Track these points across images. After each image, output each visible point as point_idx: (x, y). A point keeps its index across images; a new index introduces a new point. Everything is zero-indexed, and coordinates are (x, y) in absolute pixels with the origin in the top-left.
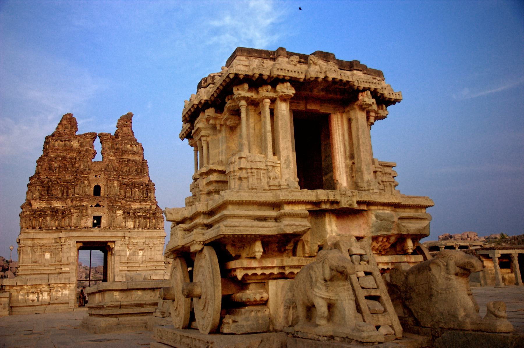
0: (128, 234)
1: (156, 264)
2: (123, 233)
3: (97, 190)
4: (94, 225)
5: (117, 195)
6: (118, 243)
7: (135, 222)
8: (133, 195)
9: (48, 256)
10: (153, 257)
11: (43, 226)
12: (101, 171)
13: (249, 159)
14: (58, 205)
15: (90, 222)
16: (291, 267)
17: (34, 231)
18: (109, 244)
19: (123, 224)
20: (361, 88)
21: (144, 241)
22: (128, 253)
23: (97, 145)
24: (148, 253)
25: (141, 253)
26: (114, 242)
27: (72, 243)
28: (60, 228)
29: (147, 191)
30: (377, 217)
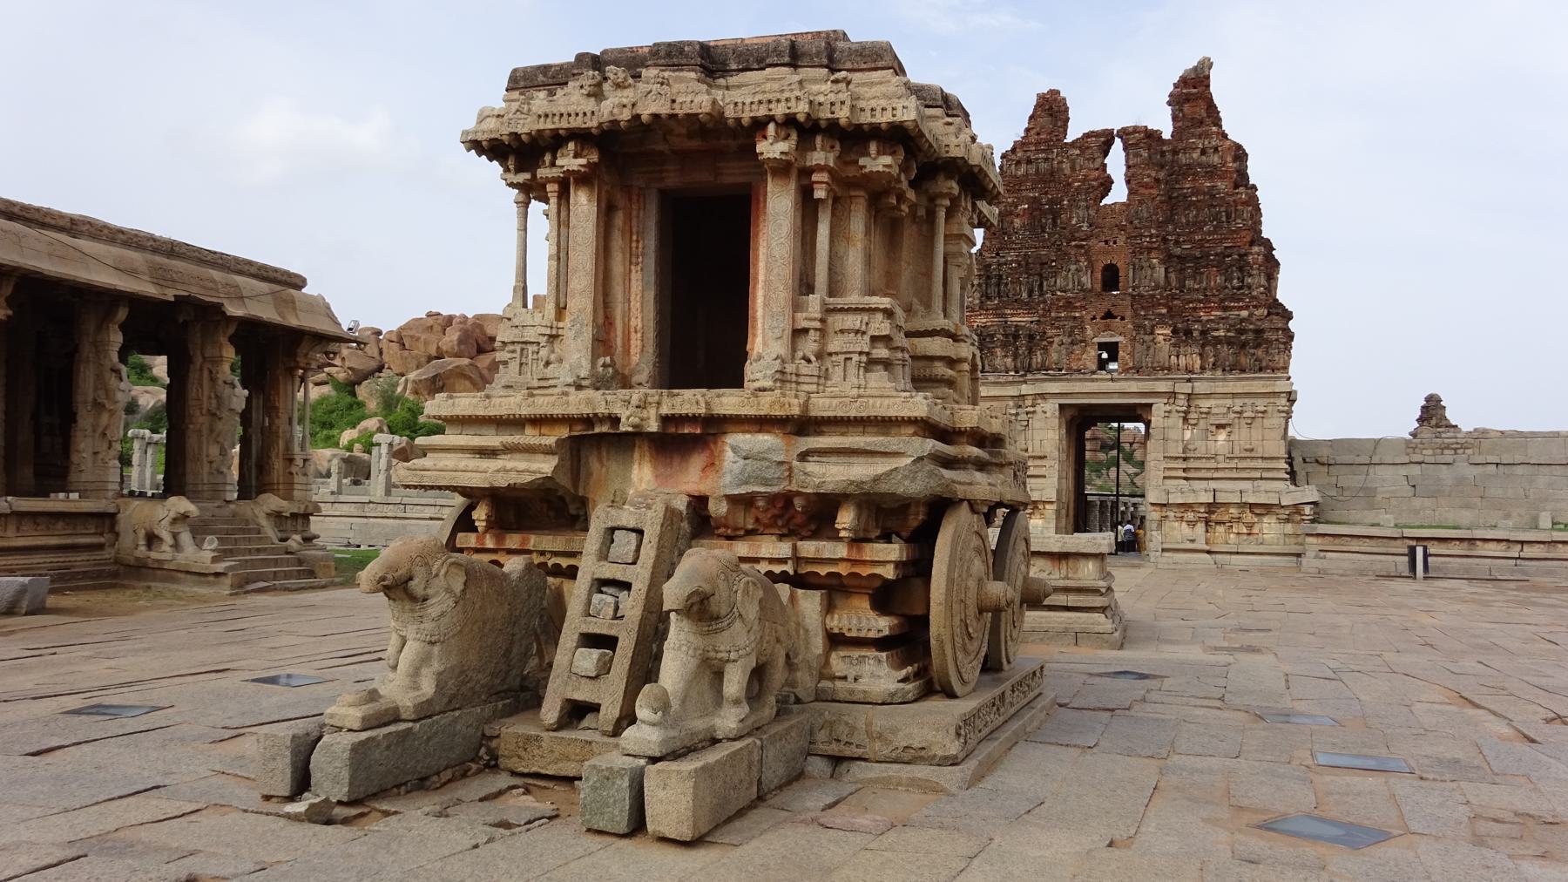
0: (1185, 388)
1: (1260, 464)
3: (1111, 278)
4: (1102, 365)
6: (1159, 408)
7: (1201, 355)
10: (1255, 444)
12: (1122, 228)
13: (516, 321)
14: (1021, 319)
15: (1090, 357)
16: (555, 554)
20: (745, 122)
22: (1188, 435)
23: (1116, 162)
24: (1244, 437)
25: (1222, 436)
27: (1051, 407)
30: (734, 449)
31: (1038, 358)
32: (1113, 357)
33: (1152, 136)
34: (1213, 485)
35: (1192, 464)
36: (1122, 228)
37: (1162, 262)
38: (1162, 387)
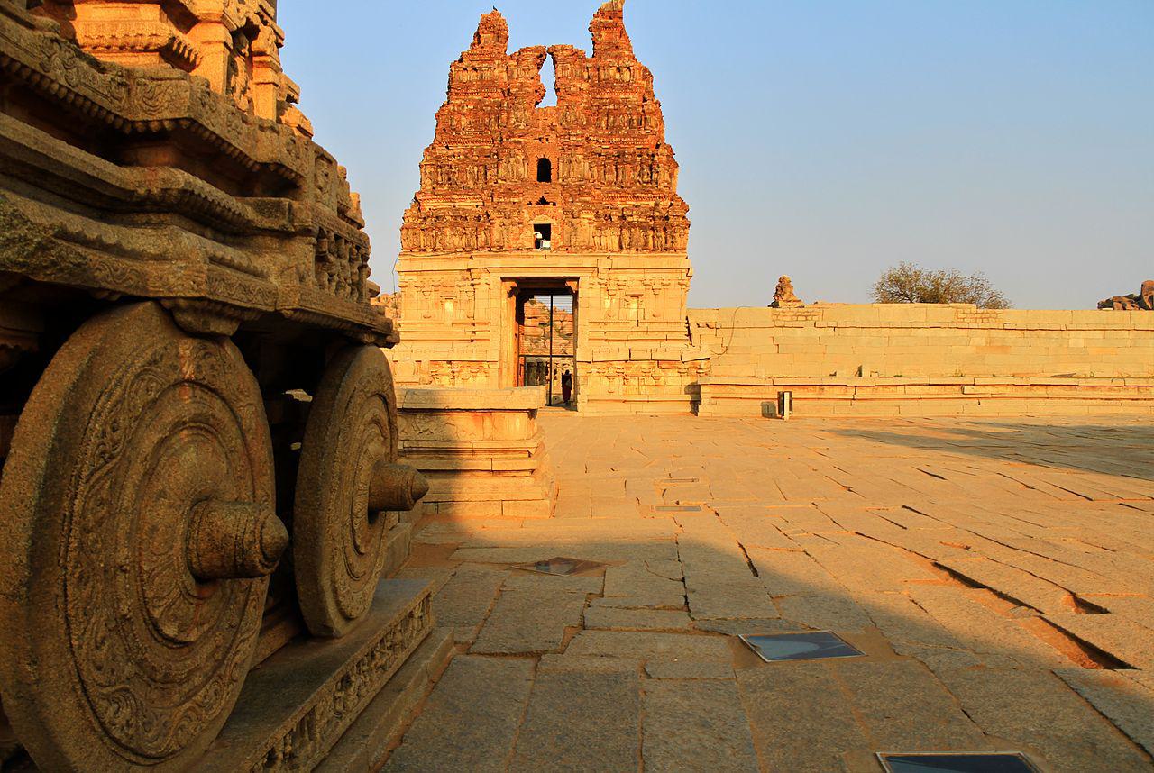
0: (605, 263)
2: (595, 259)
3: (544, 171)
5: (582, 179)
8: (620, 179)
9: (449, 306)
11: (438, 245)
14: (469, 204)
17: (423, 254)
18: (568, 283)
19: (597, 239)
21: (641, 276)
23: (548, 74)
24: (651, 303)
25: (634, 304)
26: (577, 279)
27: (495, 278)
28: (469, 250)
29: (651, 169)
31: (482, 237)
32: (547, 236)
33: (576, 55)
34: (629, 345)
35: (607, 328)
36: (552, 128)
37: (586, 158)
38: (588, 262)
